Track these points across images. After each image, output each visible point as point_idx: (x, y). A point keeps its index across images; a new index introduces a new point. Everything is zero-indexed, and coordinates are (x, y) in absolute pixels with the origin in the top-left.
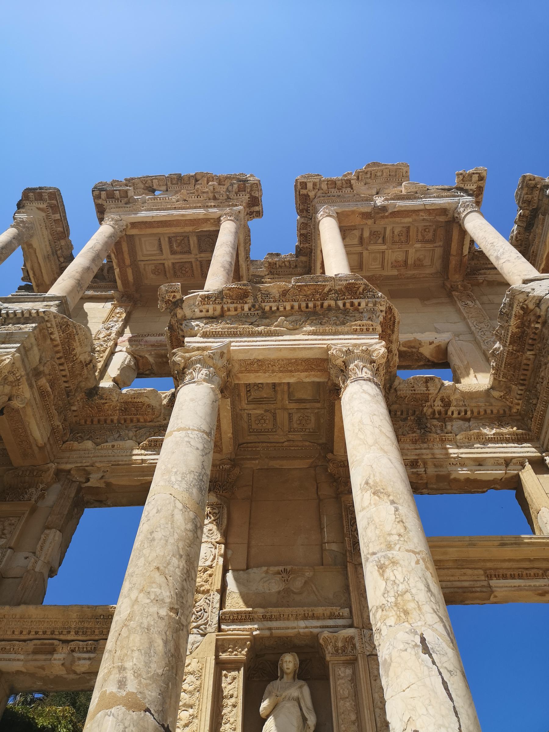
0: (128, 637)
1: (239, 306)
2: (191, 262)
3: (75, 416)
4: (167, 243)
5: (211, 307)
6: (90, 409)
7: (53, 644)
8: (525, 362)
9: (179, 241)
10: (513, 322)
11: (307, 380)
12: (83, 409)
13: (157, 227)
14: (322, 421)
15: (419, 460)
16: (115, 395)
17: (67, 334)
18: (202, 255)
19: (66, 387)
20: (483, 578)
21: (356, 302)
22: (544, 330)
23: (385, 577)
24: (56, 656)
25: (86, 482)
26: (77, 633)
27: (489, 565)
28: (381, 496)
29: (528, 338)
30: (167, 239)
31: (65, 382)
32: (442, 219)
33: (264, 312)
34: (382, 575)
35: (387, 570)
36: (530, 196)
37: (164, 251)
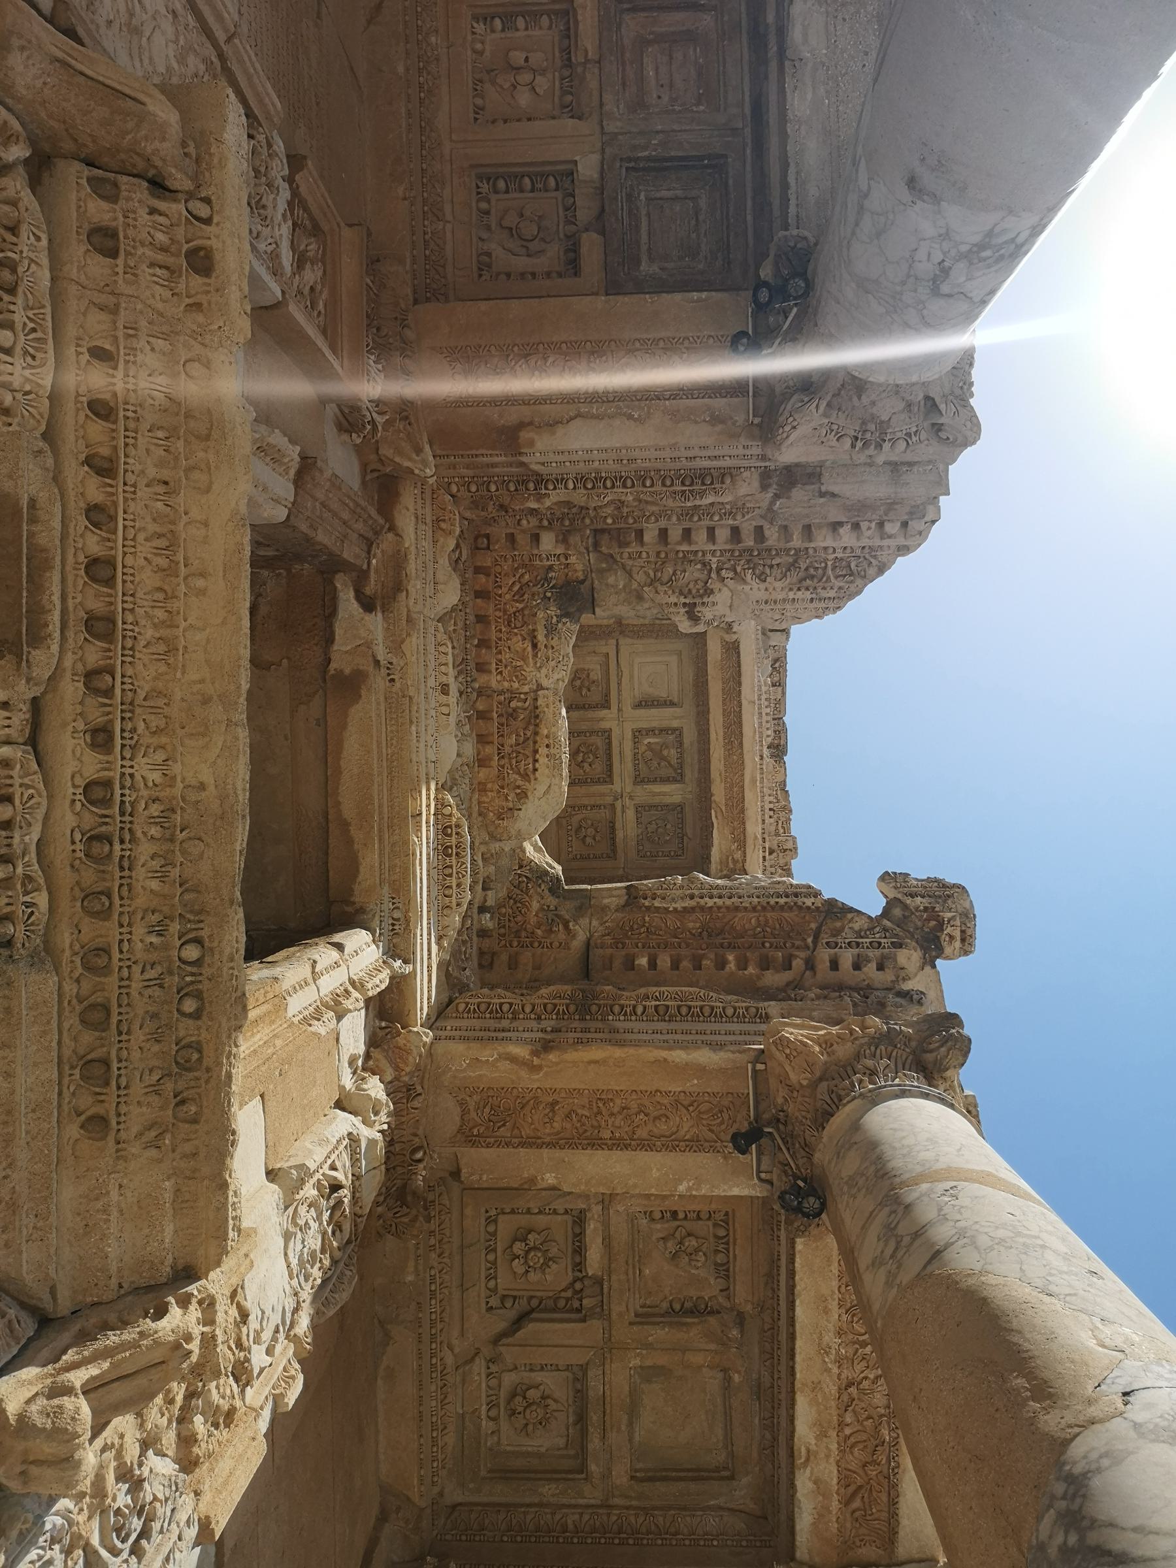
2: (608, 778)
3: (511, 538)
4: (665, 724)
6: (516, 588)
9: (665, 753)
12: (524, 566)
13: (724, 710)
14: (548, 1491)
16: (556, 676)
17: (826, 567)
18: (631, 814)
19: (640, 533)
25: (360, 596)
30: (675, 724)
31: (663, 534)
37: (641, 712)
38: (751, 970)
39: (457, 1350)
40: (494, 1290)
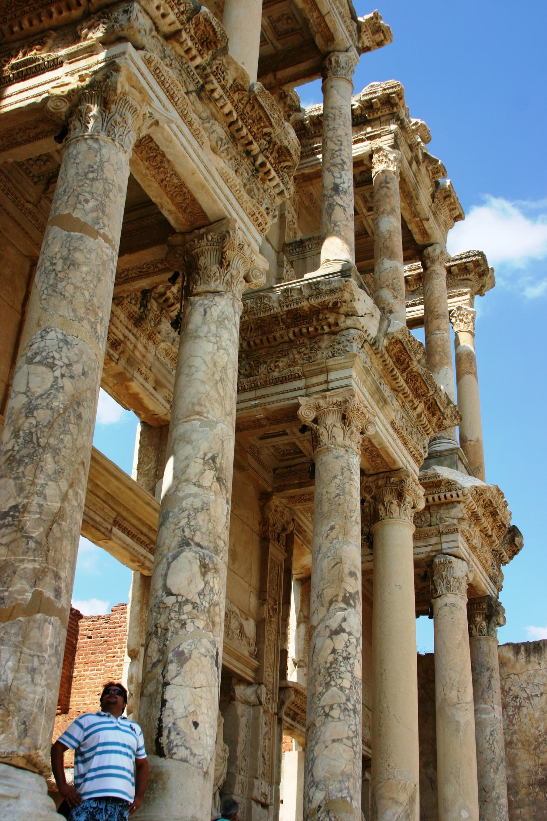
0: (60, 539)
1: (194, 52)
5: (172, 17)
8: (278, 335)
10: (314, 302)
11: (166, 214)
15: (122, 345)
20: (111, 521)
21: (273, 173)
22: (326, 337)
23: (206, 579)
27: (125, 514)
28: (223, 487)
29: (307, 325)
32: (319, 41)
33: (203, 86)
34: (204, 574)
35: (209, 573)
36: (379, 105)
38: (65, 14)
39: (32, 201)
40: (34, 176)
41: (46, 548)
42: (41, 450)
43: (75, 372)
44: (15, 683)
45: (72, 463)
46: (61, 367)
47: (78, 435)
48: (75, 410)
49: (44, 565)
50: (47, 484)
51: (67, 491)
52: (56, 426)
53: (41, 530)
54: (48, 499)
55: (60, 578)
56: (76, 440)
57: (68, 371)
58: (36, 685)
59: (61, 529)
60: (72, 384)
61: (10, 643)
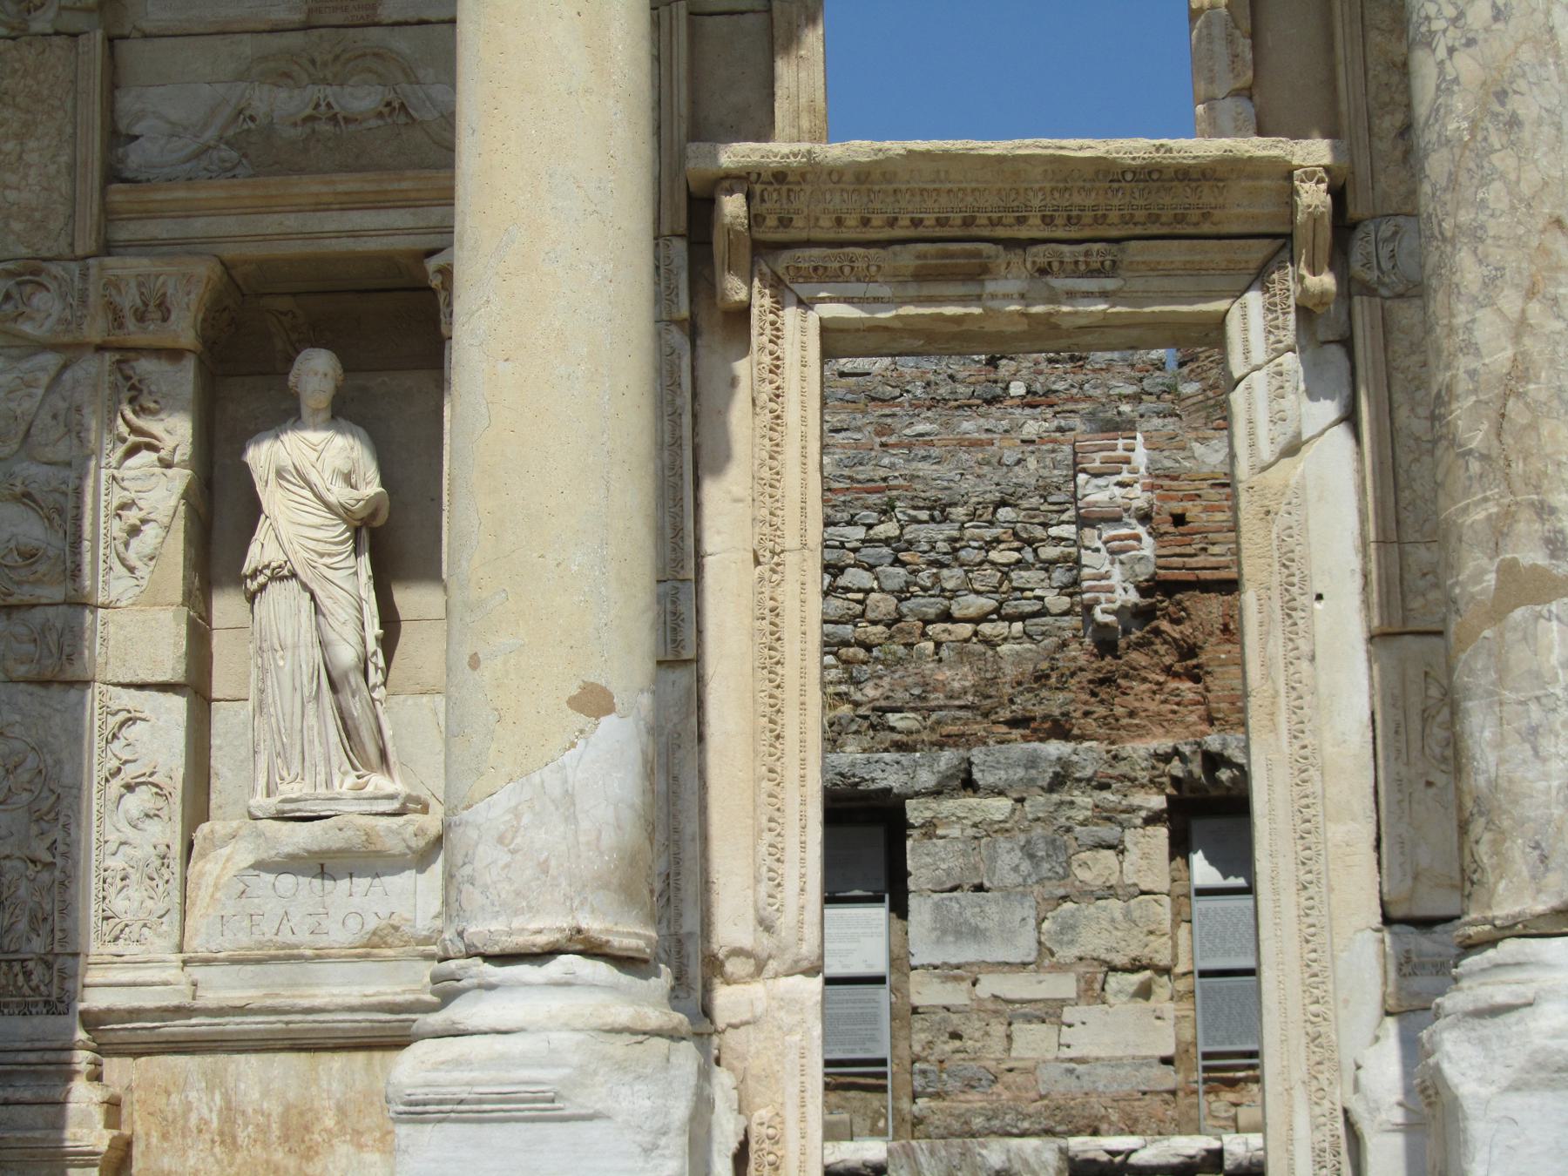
0: (1533, 426)
7: (978, 254)
24: (991, 287)
26: (1048, 221)
41: (1502, 463)
42: (1449, 249)
43: (1475, 27)
44: (1502, 770)
45: (1519, 243)
46: (1445, 31)
47: (1519, 168)
48: (1498, 115)
49: (1506, 501)
50: (1473, 321)
51: (1523, 311)
52: (1463, 177)
53: (1485, 426)
54: (1484, 351)
55: (1553, 511)
56: (1518, 181)
57: (1459, 33)
58: (1544, 760)
59: (1527, 405)
60: (1473, 58)
61: (1480, 691)
